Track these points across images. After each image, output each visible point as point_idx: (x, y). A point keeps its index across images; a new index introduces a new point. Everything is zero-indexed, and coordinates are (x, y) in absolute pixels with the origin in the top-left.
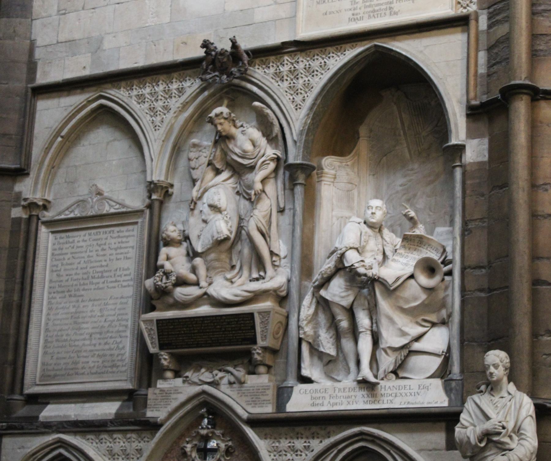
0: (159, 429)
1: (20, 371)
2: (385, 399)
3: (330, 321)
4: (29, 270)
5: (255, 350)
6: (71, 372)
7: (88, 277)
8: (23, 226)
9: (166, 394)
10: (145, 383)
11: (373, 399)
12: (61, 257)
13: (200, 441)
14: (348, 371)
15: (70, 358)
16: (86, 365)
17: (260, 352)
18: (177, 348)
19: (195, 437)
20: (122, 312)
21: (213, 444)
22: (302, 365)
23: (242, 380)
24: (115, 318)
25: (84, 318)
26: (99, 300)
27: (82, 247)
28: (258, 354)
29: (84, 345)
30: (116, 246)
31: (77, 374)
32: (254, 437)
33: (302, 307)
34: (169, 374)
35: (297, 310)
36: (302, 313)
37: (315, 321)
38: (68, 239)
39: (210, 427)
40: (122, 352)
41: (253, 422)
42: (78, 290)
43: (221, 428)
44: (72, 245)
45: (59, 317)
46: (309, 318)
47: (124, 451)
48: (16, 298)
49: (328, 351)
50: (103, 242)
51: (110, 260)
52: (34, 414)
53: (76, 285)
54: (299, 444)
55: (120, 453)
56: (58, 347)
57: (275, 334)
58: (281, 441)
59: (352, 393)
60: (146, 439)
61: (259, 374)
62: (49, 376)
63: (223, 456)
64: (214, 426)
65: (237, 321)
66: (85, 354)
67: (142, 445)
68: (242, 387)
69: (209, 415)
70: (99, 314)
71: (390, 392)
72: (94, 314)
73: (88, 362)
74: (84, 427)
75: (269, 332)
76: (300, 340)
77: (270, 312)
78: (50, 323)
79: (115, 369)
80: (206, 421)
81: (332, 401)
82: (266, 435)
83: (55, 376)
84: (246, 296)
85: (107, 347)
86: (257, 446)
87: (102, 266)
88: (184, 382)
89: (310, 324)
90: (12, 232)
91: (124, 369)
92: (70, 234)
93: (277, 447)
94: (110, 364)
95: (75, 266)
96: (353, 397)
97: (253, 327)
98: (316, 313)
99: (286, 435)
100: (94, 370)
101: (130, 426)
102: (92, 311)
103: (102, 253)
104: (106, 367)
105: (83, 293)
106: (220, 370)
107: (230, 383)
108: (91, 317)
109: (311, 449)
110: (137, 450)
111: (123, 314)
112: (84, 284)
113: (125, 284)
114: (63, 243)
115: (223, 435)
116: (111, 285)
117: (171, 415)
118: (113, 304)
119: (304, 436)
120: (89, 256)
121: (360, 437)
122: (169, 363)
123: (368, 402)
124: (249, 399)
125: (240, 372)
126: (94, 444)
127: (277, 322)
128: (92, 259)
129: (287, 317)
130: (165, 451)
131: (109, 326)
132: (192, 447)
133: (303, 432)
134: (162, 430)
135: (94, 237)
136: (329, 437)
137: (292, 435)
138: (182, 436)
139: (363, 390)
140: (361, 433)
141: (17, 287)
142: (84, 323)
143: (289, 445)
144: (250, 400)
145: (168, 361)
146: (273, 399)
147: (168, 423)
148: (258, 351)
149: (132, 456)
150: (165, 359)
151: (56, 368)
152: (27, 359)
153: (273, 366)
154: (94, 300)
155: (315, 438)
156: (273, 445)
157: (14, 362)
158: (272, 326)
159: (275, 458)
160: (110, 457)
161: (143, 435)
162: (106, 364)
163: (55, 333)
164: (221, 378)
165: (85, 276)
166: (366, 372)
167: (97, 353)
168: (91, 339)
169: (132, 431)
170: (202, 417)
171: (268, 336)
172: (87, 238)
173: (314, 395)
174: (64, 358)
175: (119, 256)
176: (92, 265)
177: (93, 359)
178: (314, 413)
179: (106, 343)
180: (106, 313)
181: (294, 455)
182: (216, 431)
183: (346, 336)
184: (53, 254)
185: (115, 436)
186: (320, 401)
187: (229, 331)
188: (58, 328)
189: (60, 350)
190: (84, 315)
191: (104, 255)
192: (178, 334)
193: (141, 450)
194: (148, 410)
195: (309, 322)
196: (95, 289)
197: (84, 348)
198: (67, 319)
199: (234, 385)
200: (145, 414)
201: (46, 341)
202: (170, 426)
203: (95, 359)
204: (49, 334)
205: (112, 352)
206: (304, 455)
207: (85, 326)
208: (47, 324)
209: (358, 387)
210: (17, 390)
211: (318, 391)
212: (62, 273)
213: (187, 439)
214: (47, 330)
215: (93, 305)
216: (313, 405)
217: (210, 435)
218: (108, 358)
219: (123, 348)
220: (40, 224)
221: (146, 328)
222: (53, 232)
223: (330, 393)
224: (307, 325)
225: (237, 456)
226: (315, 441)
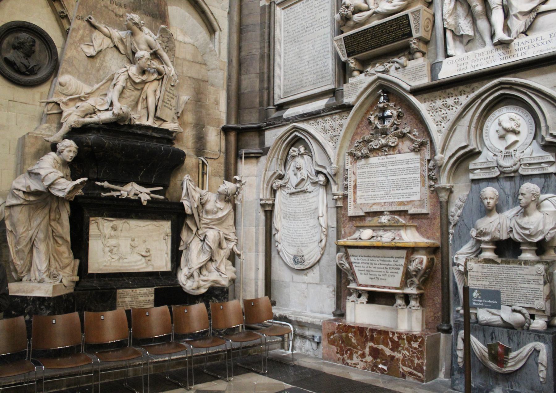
0: (351, 110)
1: (272, 92)
2: (519, 53)
3: (467, 11)
4: (272, 34)
5: (412, 41)
6: (299, 87)
7: (304, 28)
8: (267, 10)
9: (355, 85)
10: (342, 82)
11: (508, 55)
12: (289, 21)
13: (379, 112)
14: (484, 44)
15: (298, 78)
16: (307, 81)
17: (416, 42)
18: (358, 54)
19: (376, 110)
20: (325, 43)
21: (388, 113)
22: (448, 48)
23: (405, 64)
24: (321, 48)
25: (304, 53)
26: (312, 40)
27: (299, 12)
28: (414, 43)
29: (305, 69)
30: (318, 5)
31: (302, 87)
32: (416, 102)
33: (444, 4)
34: (356, 73)
35: (440, 8)
36: (444, 9)
37: (455, 14)
38: (291, 10)
39: (385, 101)
40: (327, 68)
41: (416, 92)
42: (300, 37)
43: (393, 102)
44: (294, 13)
45: (290, 56)
46: (450, 12)
47: (332, 127)
48: (266, 50)
49: (467, 33)
50: (311, 5)
51: (315, 14)
52: (280, 115)
53: (298, 35)
54: (450, 101)
55: (330, 129)
56: (291, 74)
57: (426, 29)
58: (437, 101)
59: (490, 55)
60: (345, 117)
61: (417, 58)
62: (288, 92)
63: (396, 120)
64: (388, 101)
65: (397, 24)
66: (306, 74)
67: (343, 121)
68: (405, 69)
69: (384, 94)
70: (312, 48)
71: (523, 46)
72: (309, 49)
73: (308, 79)
74: (307, 117)
75: (421, 25)
76: (445, 29)
77: (420, 10)
78: (286, 61)
79: (324, 79)
80: (382, 98)
81: (474, 64)
82: (425, 99)
83: (291, 91)
84: (401, 5)
85: (318, 67)
86: (419, 107)
87: (311, 19)
88: (366, 75)
89: (451, 17)
90: (261, 14)
91: (329, 78)
92: (292, 7)
93: (434, 106)
94: (321, 76)
95: (296, 25)
96: (491, 58)
97: (409, 25)
98: (455, 8)
99: (440, 96)
100: (312, 83)
101: (334, 110)
102: (308, 48)
103: (310, 12)
104: (318, 79)
105: (302, 38)
106: (389, 63)
107: (397, 69)
108: (308, 51)
109: (460, 103)
110: (340, 125)
111: (326, 44)
112: (302, 33)
113: (325, 26)
114: (289, 13)
115: (395, 106)
116: (317, 29)
117: (358, 98)
118: (320, 40)
119: (453, 95)
120: (304, 16)
121: (499, 87)
122: (355, 65)
123: (505, 58)
124: (411, 76)
125: (403, 60)
126: (314, 126)
127: (426, 18)
128: (305, 17)
129: (434, 15)
130: (358, 123)
131: (318, 54)
132: (375, 117)
133: (452, 92)
134: (354, 109)
135: (305, 4)
136: (473, 92)
137: (444, 96)
138: (368, 111)
139: (499, 50)
140: (501, 83)
141: (266, 44)
142: (304, 56)
143: (443, 103)
144: (412, 77)
145: (354, 64)
146: (428, 73)
147: (357, 103)
148: (414, 41)
149: (337, 130)
150: (352, 63)
151: (291, 86)
152: (275, 85)
153: (426, 52)
154: (309, 41)
155: (463, 94)
156: (431, 105)
157: (268, 88)
158: (423, 21)
159: (433, 114)
160: (324, 132)
161: (343, 115)
162: (318, 77)
163: (289, 66)
164: (390, 67)
165: (302, 29)
166: (501, 35)
167: (312, 72)
168: (308, 65)
169: (336, 113)
170: (380, 96)
171: (420, 29)
172: (302, 5)
173: (459, 63)
174: (295, 80)
175: (320, 11)
176: (306, 20)
177: (311, 76)
178: (461, 76)
179: (317, 65)
180: (316, 46)
181: (447, 110)
182: (389, 104)
183: (481, 17)
184: (284, 21)
185: (326, 119)
186: (465, 66)
187: (392, 32)
188: (290, 63)
189: (292, 75)
190: (304, 51)
191: (312, 13)
192: (358, 44)
193: (342, 125)
194: (344, 98)
195: (450, 15)
196: (308, 34)
197: (305, 71)
198: (295, 56)
199: (399, 70)
200: (343, 101)
201: (285, 72)
202: (358, 105)
203: (312, 76)
204: (286, 68)
205: (321, 69)
206: (454, 108)
207: (304, 58)
208: (284, 62)
209: (494, 49)
210: (272, 104)
211: (462, 59)
212: (290, 30)
213: (371, 113)
214: (285, 66)
215: (308, 44)
216: (459, 70)
217: (386, 107)
218: (319, 73)
219: (328, 65)
220: (276, 6)
221: (338, 45)
222: (283, 9)
223: (472, 59)
224: (449, 17)
225: (406, 118)
226: (462, 97)
